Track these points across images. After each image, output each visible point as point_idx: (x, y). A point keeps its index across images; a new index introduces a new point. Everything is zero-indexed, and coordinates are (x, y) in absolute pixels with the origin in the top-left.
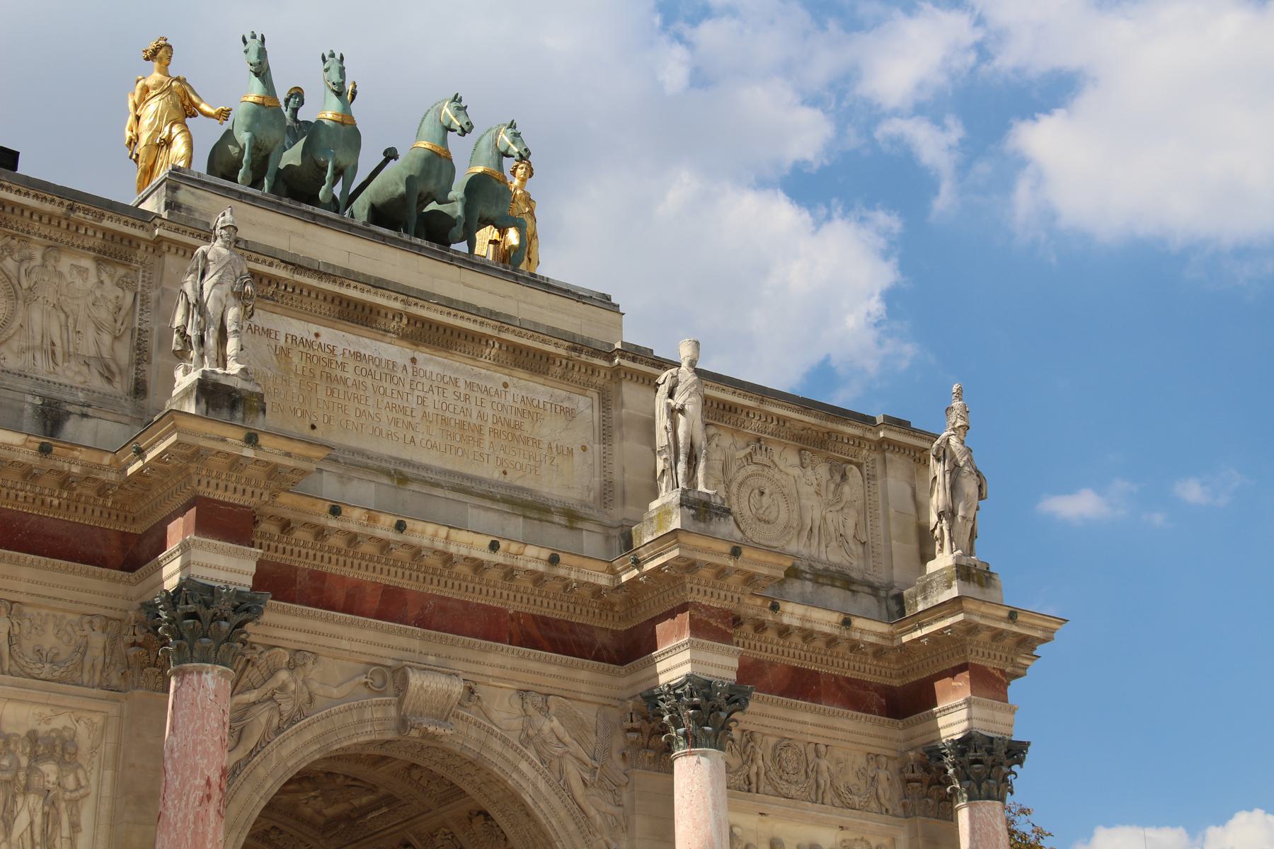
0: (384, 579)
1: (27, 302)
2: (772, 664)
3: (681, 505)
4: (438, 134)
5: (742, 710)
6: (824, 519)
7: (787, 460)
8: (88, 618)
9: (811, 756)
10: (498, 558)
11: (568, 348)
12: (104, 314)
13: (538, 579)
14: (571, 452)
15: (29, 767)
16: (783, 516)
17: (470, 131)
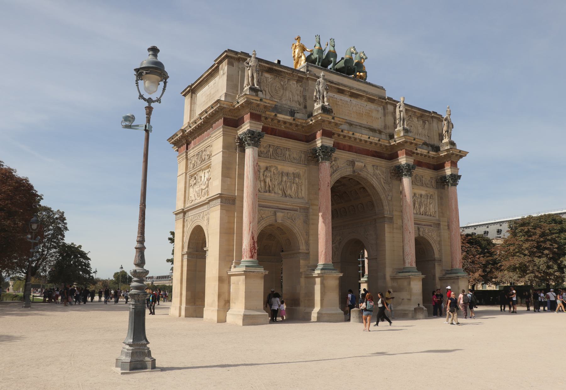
0: (349, 144)
3: (403, 130)
4: (351, 54)
5: (414, 169)
6: (422, 132)
7: (415, 120)
8: (301, 152)
9: (421, 178)
10: (369, 140)
11: (379, 98)
12: (298, 93)
13: (376, 144)
14: (378, 119)
15: (293, 179)
17: (357, 53)
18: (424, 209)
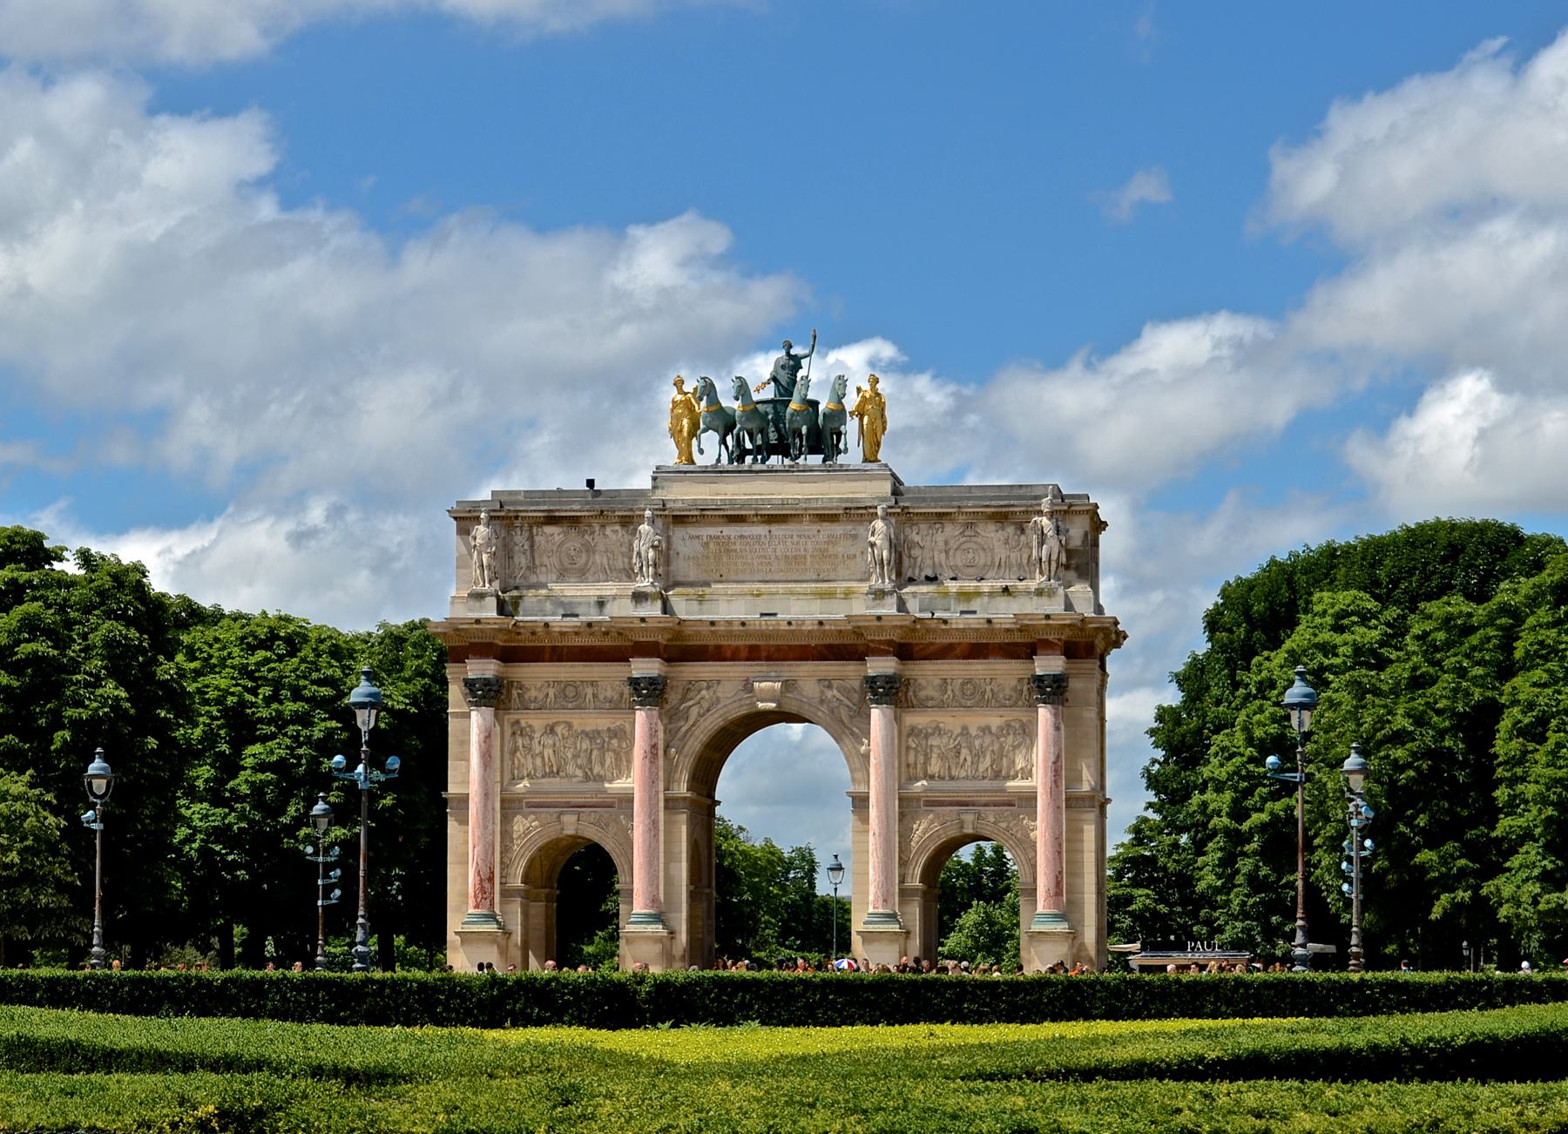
0: (747, 643)
1: (594, 553)
2: (959, 644)
14: (855, 556)
16: (982, 561)
18: (989, 763)
